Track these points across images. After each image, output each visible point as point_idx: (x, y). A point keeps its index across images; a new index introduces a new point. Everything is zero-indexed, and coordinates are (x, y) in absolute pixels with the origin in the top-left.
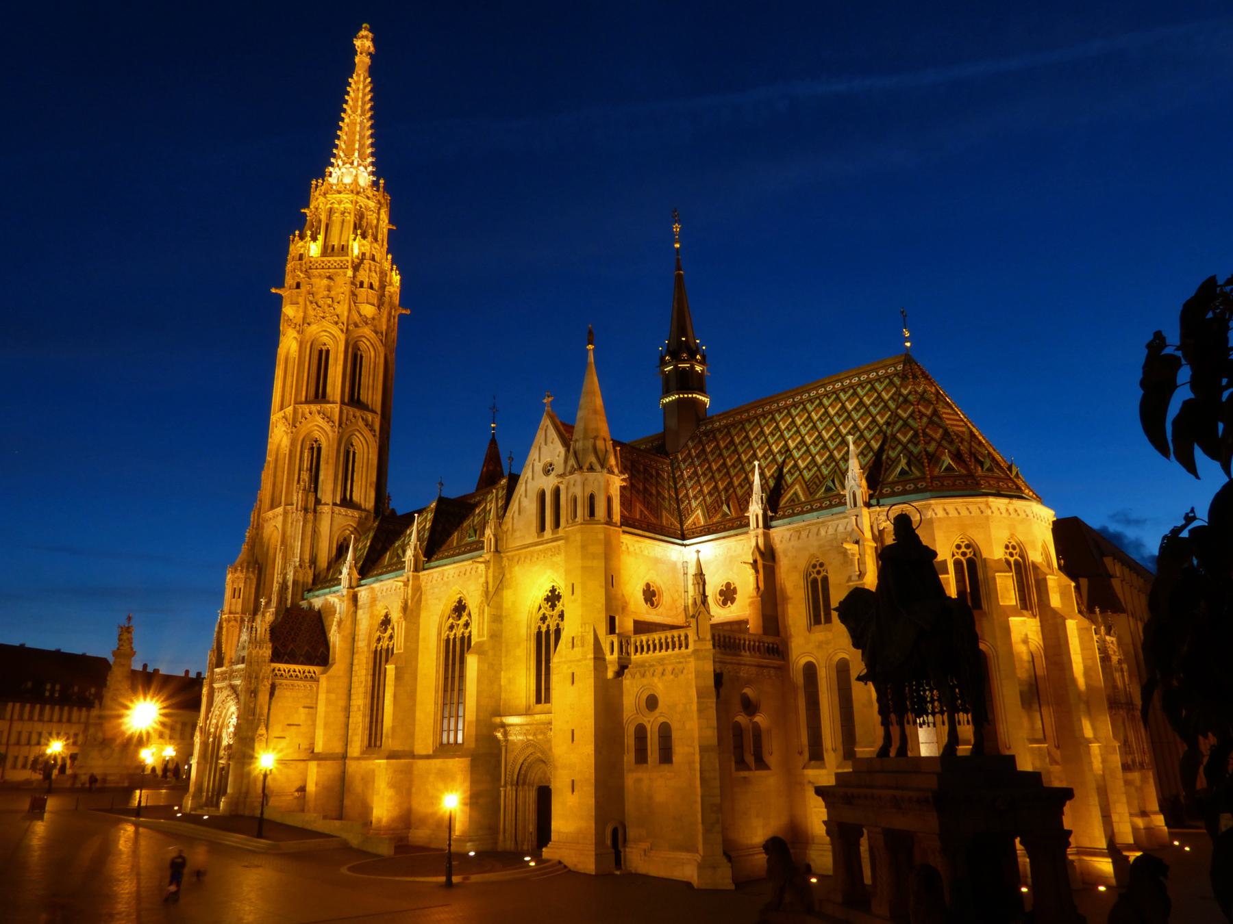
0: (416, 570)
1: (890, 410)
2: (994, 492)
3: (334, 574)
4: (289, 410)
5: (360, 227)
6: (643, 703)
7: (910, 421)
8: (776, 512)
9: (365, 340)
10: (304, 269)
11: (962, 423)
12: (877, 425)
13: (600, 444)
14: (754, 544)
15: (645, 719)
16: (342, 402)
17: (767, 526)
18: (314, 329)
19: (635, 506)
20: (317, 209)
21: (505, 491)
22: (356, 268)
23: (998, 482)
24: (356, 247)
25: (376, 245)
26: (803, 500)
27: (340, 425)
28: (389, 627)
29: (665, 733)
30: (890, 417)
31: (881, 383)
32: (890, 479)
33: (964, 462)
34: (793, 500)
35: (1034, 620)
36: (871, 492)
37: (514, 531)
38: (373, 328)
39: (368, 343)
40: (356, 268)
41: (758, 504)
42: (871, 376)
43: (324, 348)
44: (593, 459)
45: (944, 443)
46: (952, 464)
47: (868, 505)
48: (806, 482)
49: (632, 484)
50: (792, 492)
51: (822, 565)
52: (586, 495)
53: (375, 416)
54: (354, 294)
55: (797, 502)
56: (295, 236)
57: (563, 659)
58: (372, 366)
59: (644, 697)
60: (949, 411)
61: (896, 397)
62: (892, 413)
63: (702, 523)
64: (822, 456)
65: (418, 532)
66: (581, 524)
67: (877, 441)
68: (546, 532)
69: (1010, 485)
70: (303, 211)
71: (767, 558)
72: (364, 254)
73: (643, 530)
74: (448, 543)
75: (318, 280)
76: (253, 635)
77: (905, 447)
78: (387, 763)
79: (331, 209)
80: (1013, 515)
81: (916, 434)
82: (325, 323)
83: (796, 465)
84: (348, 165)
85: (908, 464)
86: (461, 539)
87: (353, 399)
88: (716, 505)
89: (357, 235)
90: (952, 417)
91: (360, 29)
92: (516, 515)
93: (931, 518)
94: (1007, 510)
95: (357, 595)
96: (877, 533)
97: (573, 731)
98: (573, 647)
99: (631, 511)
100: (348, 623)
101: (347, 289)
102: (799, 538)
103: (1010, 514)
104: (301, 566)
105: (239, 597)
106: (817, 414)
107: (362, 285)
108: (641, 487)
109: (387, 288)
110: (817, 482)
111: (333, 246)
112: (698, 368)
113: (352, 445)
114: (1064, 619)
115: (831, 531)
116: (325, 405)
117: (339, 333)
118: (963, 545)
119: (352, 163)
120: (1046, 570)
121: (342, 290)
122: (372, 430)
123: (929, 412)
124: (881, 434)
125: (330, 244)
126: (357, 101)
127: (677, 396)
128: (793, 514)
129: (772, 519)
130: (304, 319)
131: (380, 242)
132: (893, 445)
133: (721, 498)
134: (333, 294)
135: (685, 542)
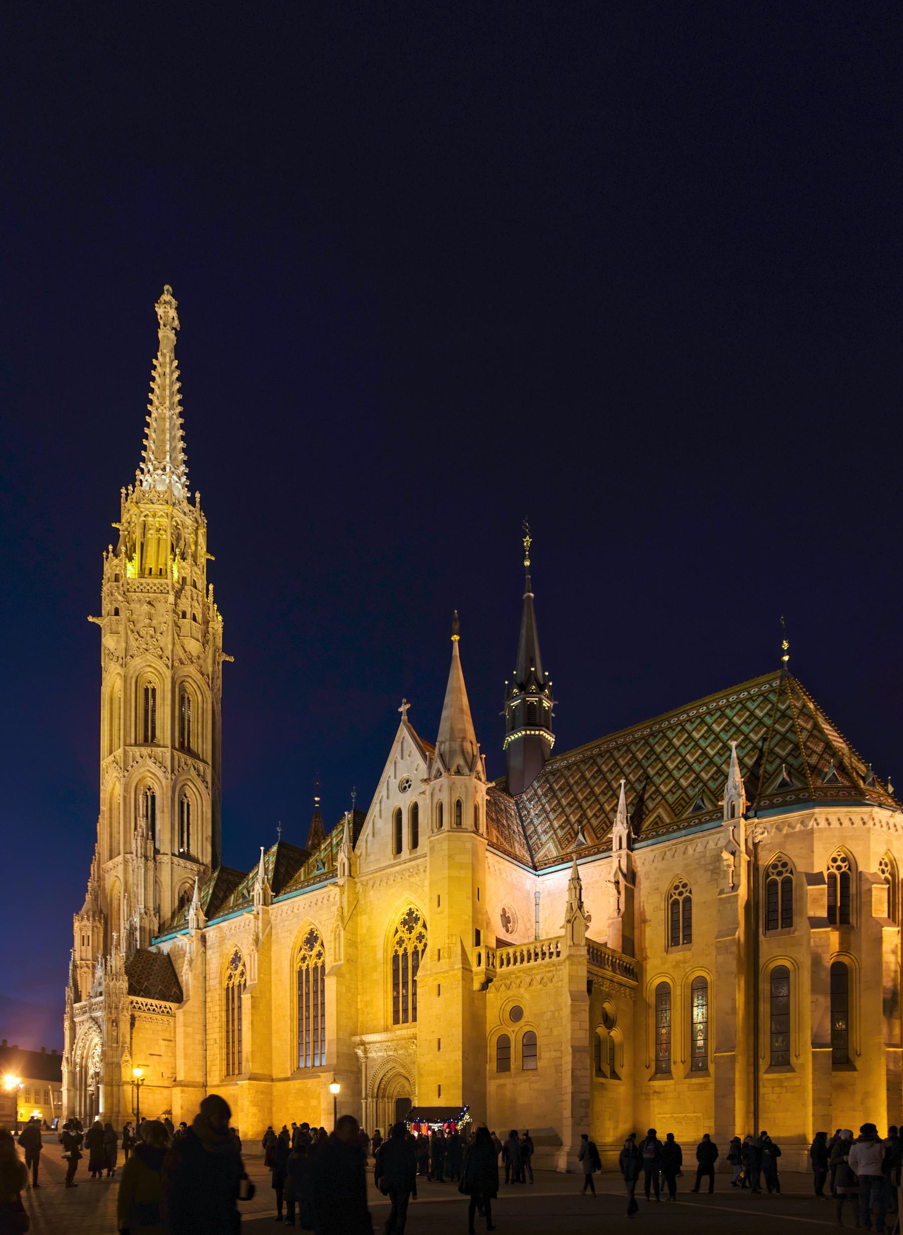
6: (507, 1014)
15: (508, 1029)
17: (631, 848)
18: (137, 663)
22: (178, 595)
24: (176, 570)
25: (196, 569)
26: (668, 821)
29: (530, 1043)
34: (657, 823)
40: (178, 595)
48: (670, 805)
51: (685, 886)
55: (660, 824)
57: (429, 972)
59: (509, 1009)
75: (138, 606)
78: (249, 1084)
82: (149, 657)
89: (175, 555)
97: (439, 1040)
100: (198, 962)
101: (169, 618)
102: (663, 859)
110: (683, 803)
121: (164, 620)
125: (147, 567)
129: (635, 841)
131: (201, 567)
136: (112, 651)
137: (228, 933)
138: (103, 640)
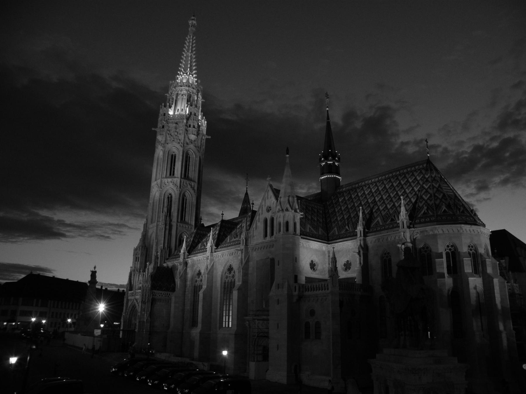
0: (212, 252)
1: (420, 185)
3: (177, 252)
4: (159, 181)
5: (190, 101)
7: (429, 190)
8: (369, 230)
9: (190, 150)
10: (166, 120)
11: (451, 191)
12: (414, 191)
13: (291, 199)
14: (359, 244)
17: (365, 235)
18: (169, 146)
20: (171, 93)
21: (250, 218)
27: (180, 187)
28: (200, 276)
29: (318, 325)
30: (420, 188)
31: (417, 172)
32: (419, 216)
34: (377, 225)
35: (480, 278)
36: (411, 222)
37: (253, 236)
38: (194, 145)
39: (192, 152)
41: (361, 226)
42: (412, 169)
43: (174, 154)
44: (288, 206)
45: (443, 200)
46: (446, 209)
47: (409, 227)
48: (382, 216)
49: (306, 216)
50: (376, 221)
51: (388, 253)
52: (285, 221)
53: (195, 183)
54: (186, 130)
56: (162, 105)
58: (194, 162)
61: (423, 179)
62: (421, 186)
63: (337, 234)
64: (390, 205)
65: (213, 235)
67: (414, 198)
68: (267, 237)
69: (471, 219)
70: (166, 94)
71: (364, 250)
72: (191, 113)
73: (310, 237)
74: (225, 241)
76: (144, 278)
77: (426, 201)
79: (177, 94)
80: (472, 232)
81: (431, 196)
82: (174, 143)
83: (378, 209)
84: (185, 74)
85: (427, 209)
86: (231, 239)
87: (185, 176)
88: (343, 225)
90: (447, 188)
92: (255, 229)
93: (436, 234)
94: (470, 230)
95: (187, 262)
96: (413, 240)
98: (278, 288)
103: (471, 232)
104: (163, 248)
105: (139, 261)
106: (388, 185)
107: (190, 126)
108: (310, 218)
109: (201, 127)
110: (388, 216)
111: (178, 109)
113: (185, 196)
114: (493, 278)
115: (393, 239)
116: (174, 179)
117: (180, 147)
118: (450, 245)
119: (187, 74)
120: (485, 256)
121: (182, 129)
122: (193, 189)
123: (437, 186)
124: (416, 196)
126: (189, 47)
128: (377, 231)
129: (367, 233)
130: (166, 141)
132: (421, 200)
133: (345, 223)
134: (178, 130)
135: (329, 242)
136: (160, 141)
137: (196, 262)
138: (157, 137)
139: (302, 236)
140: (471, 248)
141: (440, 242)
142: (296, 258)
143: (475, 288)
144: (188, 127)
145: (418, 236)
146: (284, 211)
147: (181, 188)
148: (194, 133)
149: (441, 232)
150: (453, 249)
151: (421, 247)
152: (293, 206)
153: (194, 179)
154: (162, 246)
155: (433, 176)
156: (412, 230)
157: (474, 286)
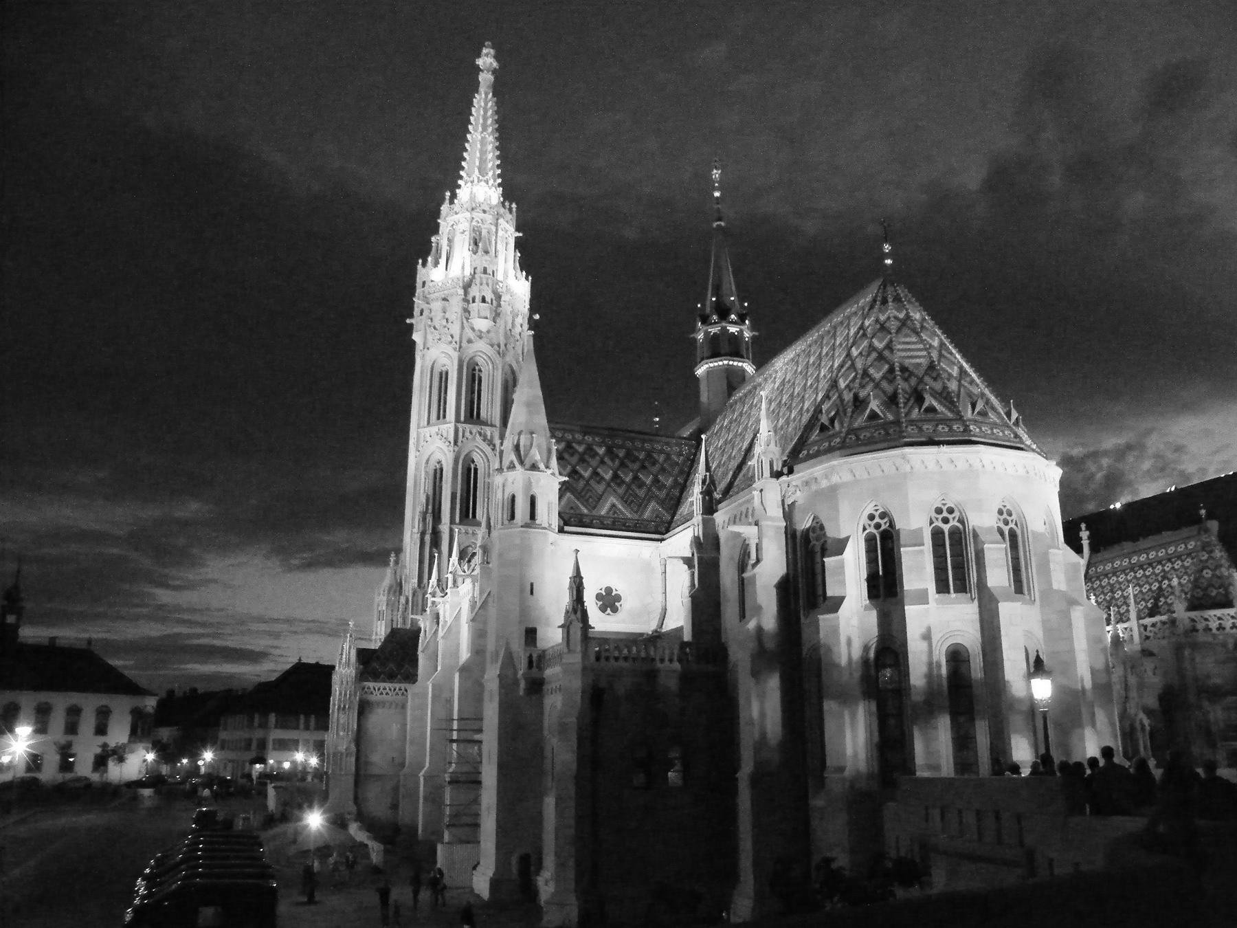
2: (923, 439)
9: (480, 354)
11: (924, 353)
16: (458, 420)
17: (710, 508)
19: (606, 501)
23: (937, 425)
33: (897, 404)
35: (970, 605)
40: (467, 287)
44: (513, 457)
45: (884, 384)
47: (777, 475)
52: (506, 498)
53: (494, 429)
54: (466, 311)
60: (914, 339)
66: (501, 529)
72: (475, 269)
81: (855, 378)
84: (469, 184)
91: (481, 46)
99: (594, 508)
112: (733, 329)
113: (473, 461)
127: (707, 366)
134: (447, 316)
135: (665, 536)
139: (566, 528)
140: (945, 514)
141: (845, 508)
142: (532, 585)
143: (927, 637)
144: (471, 302)
145: (799, 497)
146: (505, 470)
147: (457, 446)
148: (483, 314)
149: (847, 477)
150: (885, 523)
151: (807, 526)
152: (526, 455)
153: (491, 421)
154: (416, 580)
155: (882, 318)
156: (785, 482)
157: (923, 630)
